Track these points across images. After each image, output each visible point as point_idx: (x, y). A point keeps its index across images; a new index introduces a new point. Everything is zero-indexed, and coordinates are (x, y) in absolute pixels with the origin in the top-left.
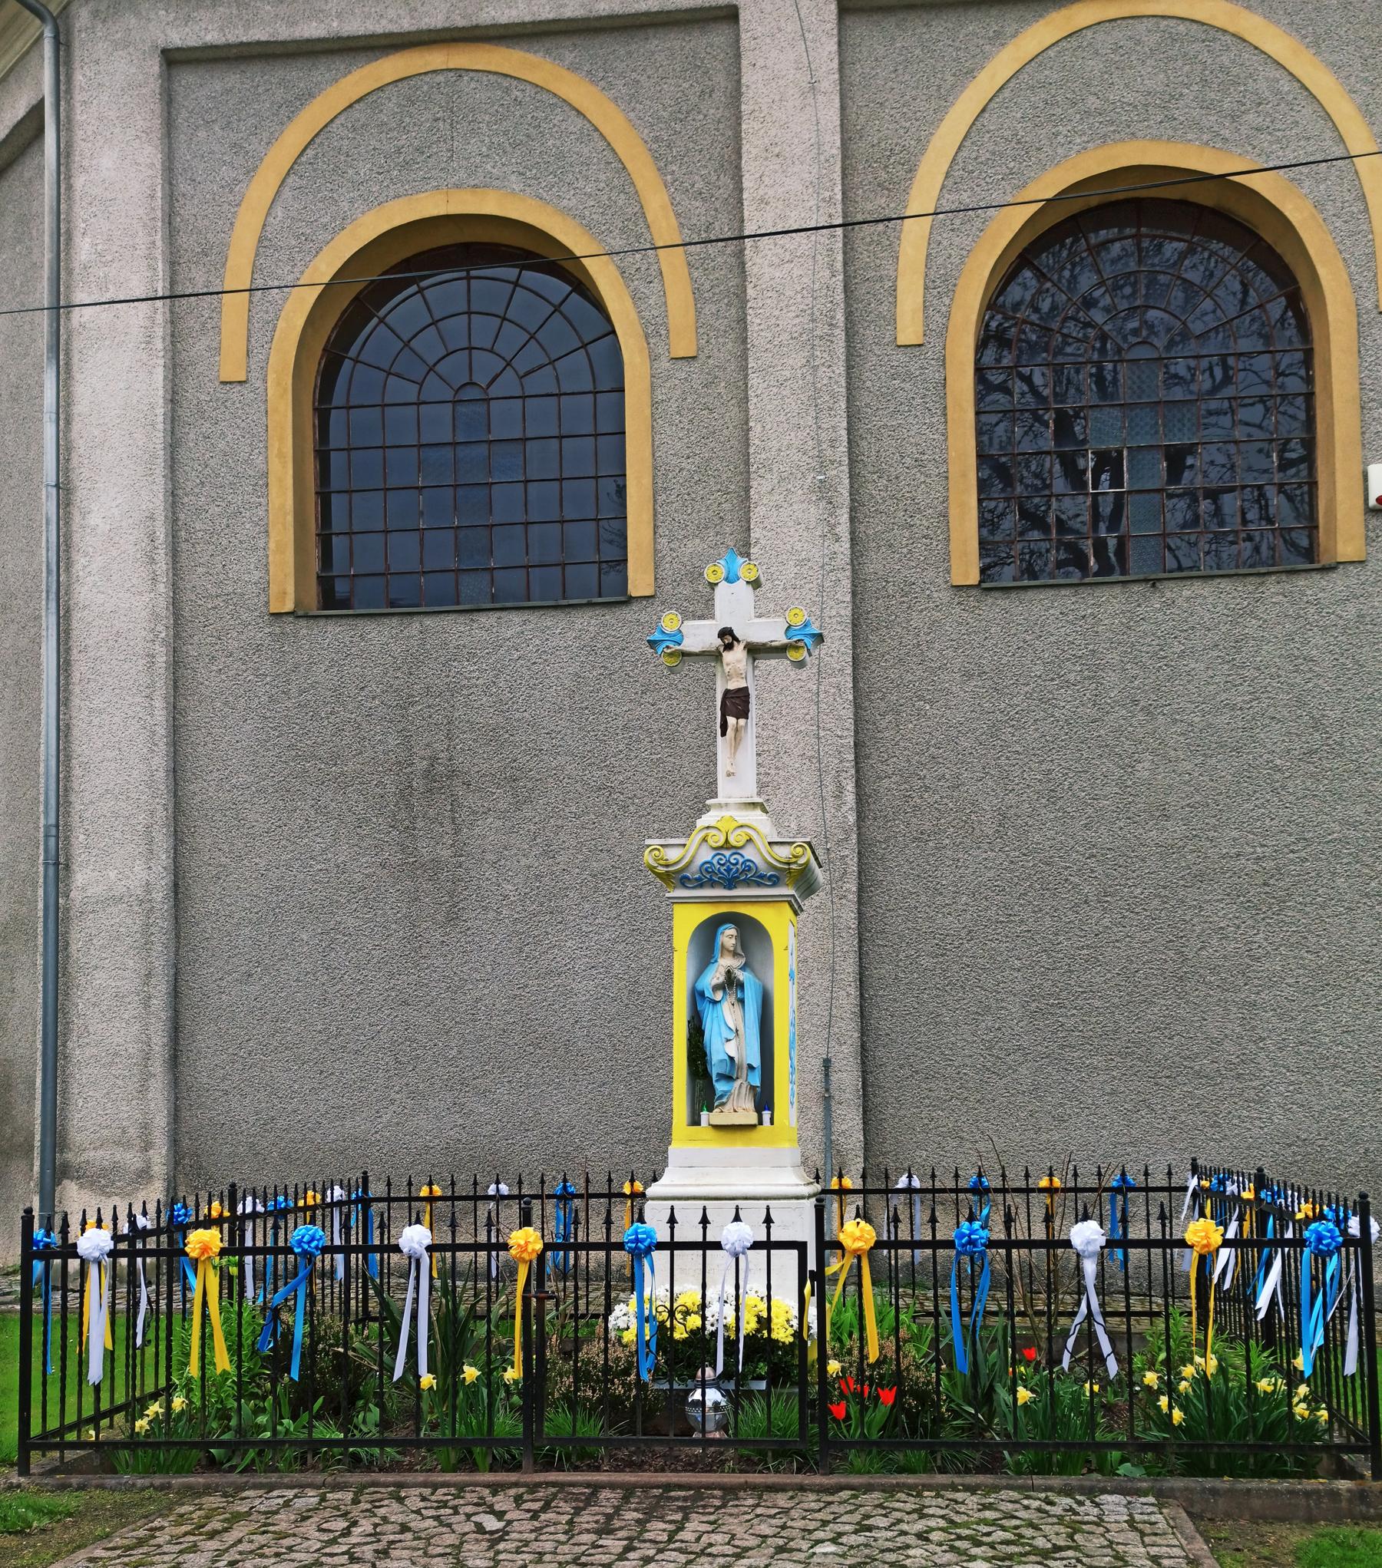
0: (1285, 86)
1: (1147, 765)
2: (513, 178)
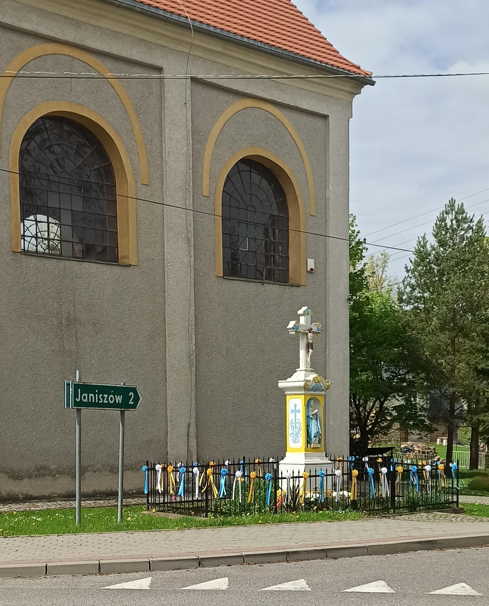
0: (292, 142)
1: (260, 338)
2: (92, 104)
